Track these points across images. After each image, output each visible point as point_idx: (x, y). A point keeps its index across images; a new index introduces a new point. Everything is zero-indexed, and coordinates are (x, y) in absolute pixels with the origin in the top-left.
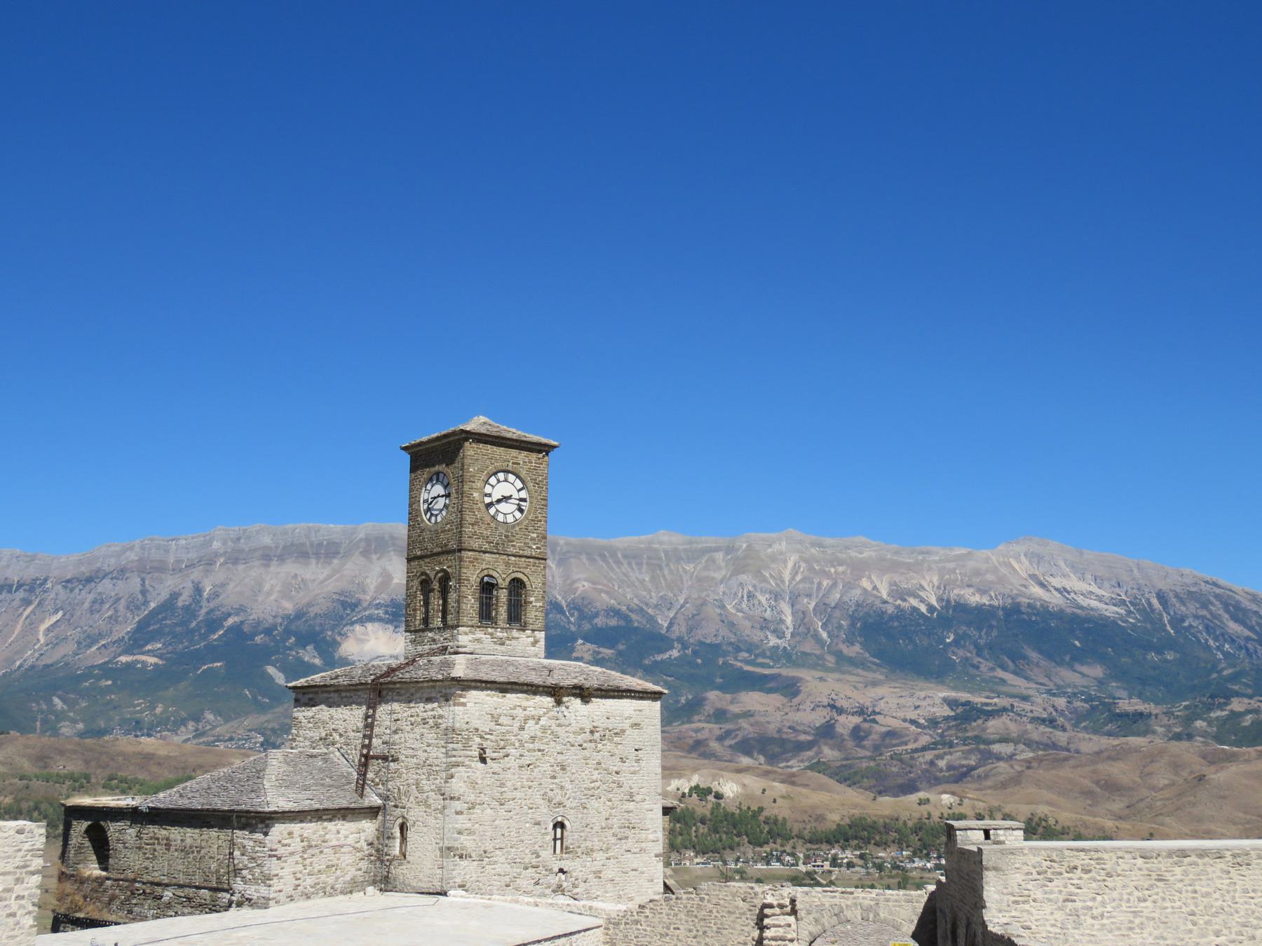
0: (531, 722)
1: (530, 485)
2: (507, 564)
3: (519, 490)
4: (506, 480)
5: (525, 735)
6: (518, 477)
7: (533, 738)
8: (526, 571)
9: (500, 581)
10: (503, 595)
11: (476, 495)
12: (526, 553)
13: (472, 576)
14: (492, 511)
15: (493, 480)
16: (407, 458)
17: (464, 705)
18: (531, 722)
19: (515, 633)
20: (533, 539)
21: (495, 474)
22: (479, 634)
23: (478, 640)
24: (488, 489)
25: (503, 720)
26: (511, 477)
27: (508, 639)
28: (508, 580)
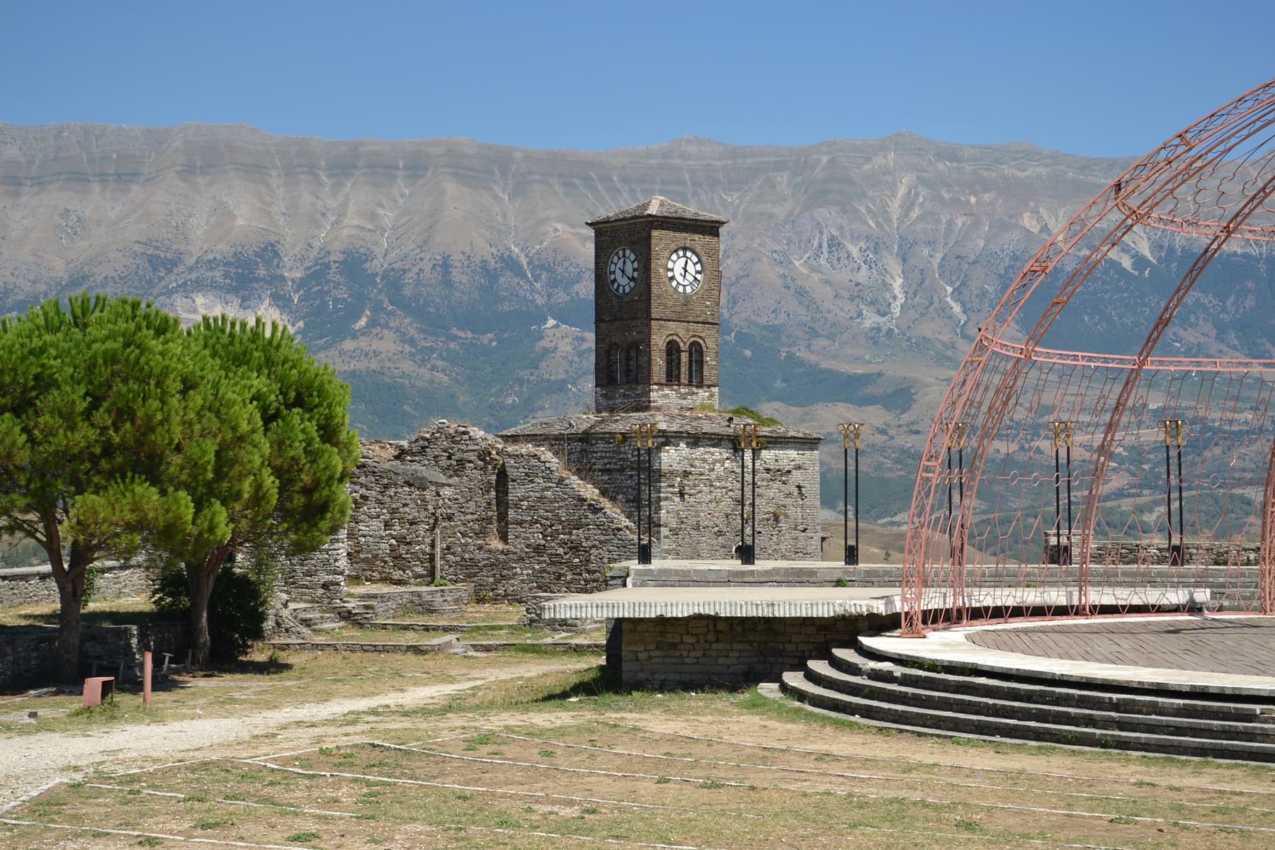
0: (718, 465)
1: (704, 259)
2: (688, 330)
6: (694, 252)
7: (719, 479)
8: (703, 335)
9: (681, 344)
10: (684, 357)
12: (700, 319)
13: (659, 341)
14: (674, 284)
15: (674, 257)
16: (591, 233)
17: (668, 452)
18: (718, 465)
19: (695, 390)
21: (676, 251)
22: (667, 391)
23: (666, 396)
24: (670, 265)
25: (697, 463)
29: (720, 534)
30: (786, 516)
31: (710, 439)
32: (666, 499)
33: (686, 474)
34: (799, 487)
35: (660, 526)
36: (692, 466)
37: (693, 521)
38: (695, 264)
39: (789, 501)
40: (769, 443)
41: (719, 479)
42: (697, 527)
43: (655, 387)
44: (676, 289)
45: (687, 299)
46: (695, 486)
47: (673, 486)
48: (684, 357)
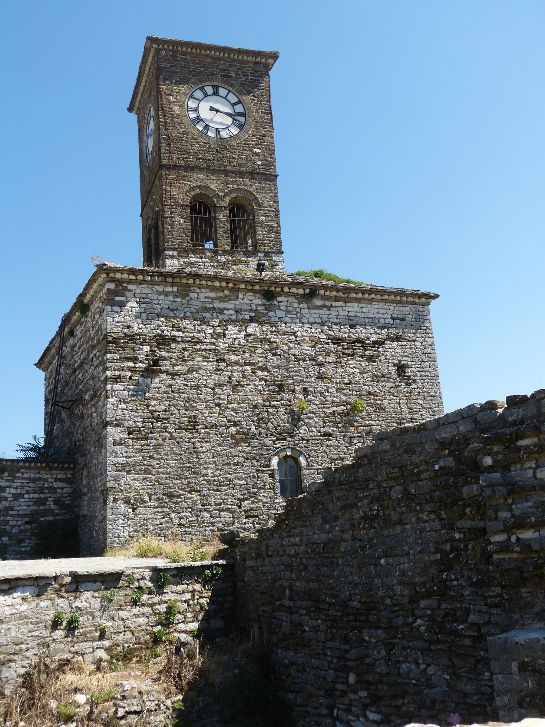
3: (233, 105)
4: (216, 93)
5: (222, 345)
10: (223, 216)
11: (175, 108)
12: (249, 168)
20: (257, 155)
26: (222, 92)
27: (234, 263)
28: (228, 199)
29: (245, 437)
30: (379, 408)
31: (213, 289)
32: (117, 380)
33: (163, 341)
34: (401, 368)
35: (106, 424)
36: (175, 328)
37: (179, 415)
38: (233, 105)
39: (379, 387)
40: (336, 299)
41: (232, 349)
42: (192, 424)
43: (171, 253)
44: (203, 134)
45: (222, 145)
46: (183, 360)
47: (135, 359)
48: (223, 216)
